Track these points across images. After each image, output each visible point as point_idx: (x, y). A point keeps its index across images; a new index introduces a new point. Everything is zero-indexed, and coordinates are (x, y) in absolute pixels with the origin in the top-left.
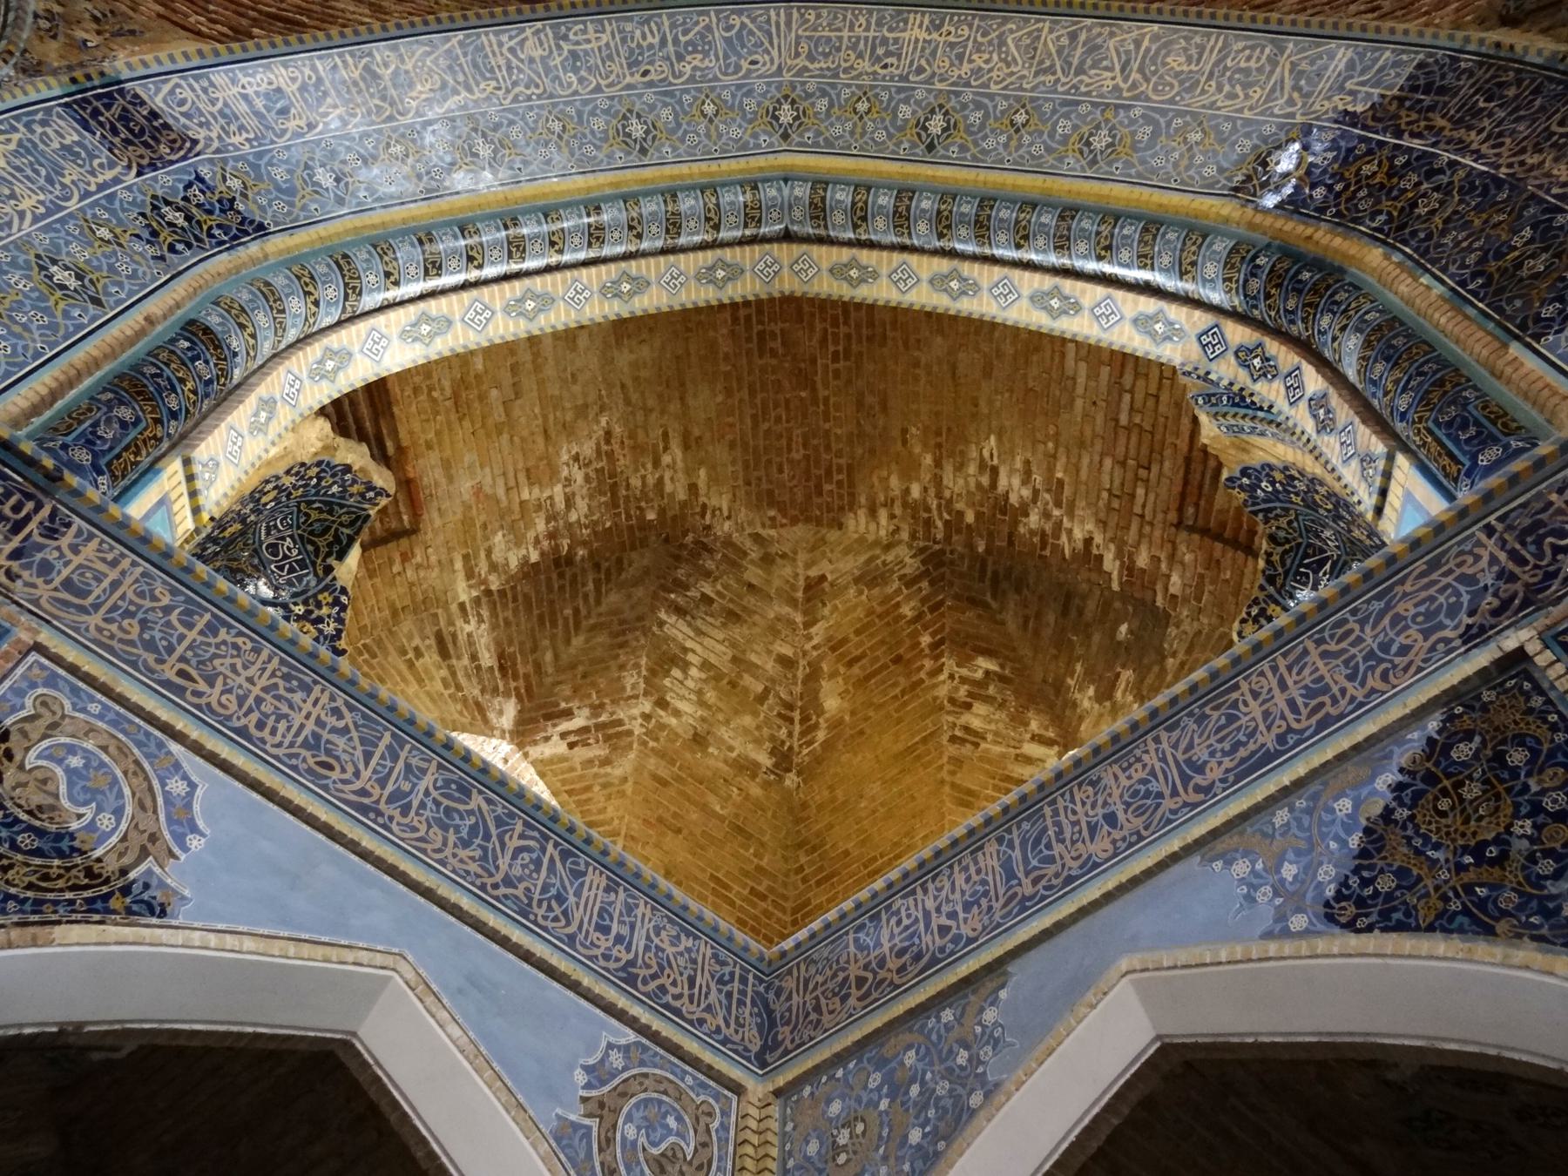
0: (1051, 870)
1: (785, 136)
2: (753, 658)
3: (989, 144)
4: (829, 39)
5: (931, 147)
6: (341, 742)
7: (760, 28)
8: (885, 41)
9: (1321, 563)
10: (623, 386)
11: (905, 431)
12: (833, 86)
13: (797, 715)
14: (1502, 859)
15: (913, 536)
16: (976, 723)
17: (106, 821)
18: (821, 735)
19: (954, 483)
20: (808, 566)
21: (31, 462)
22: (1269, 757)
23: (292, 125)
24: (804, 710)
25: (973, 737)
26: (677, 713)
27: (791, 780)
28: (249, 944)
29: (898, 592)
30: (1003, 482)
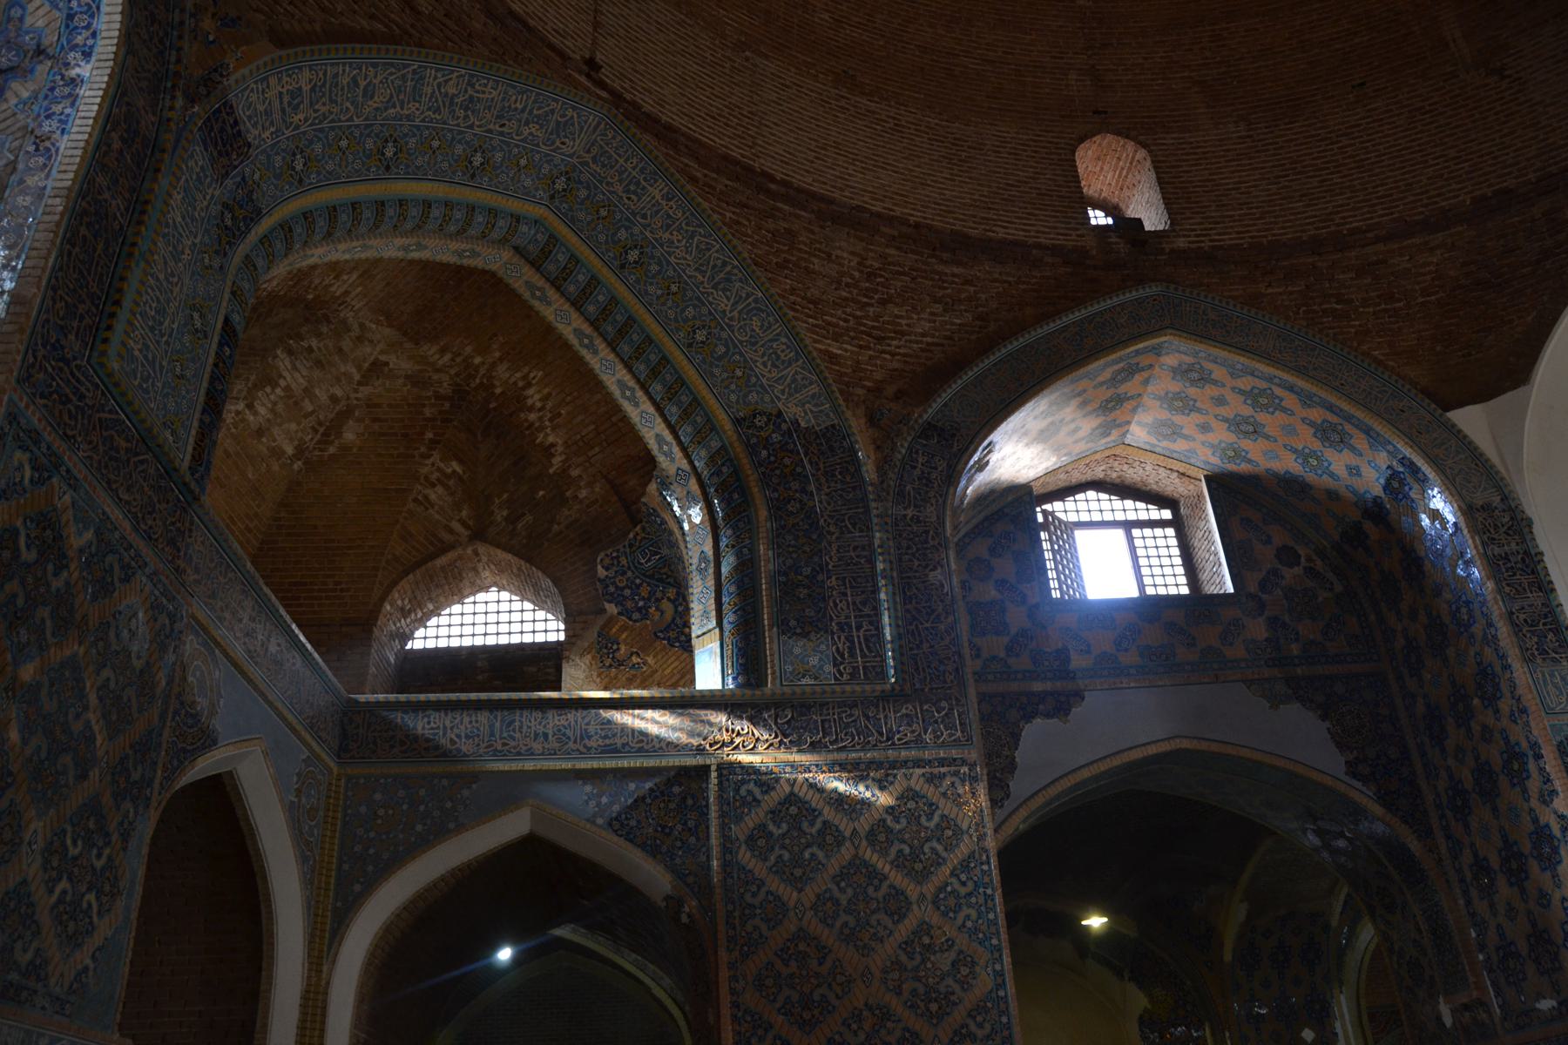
0: (513, 743)
1: (552, 197)
2: (317, 391)
3: (651, 289)
4: (610, 157)
5: (622, 266)
8: (638, 184)
9: (656, 553)
11: (495, 335)
12: (596, 188)
13: (322, 430)
14: (669, 835)
15: (457, 375)
16: (433, 497)
18: (332, 450)
19: (502, 371)
20: (382, 352)
22: (616, 751)
23: (296, 118)
24: (330, 431)
25: (427, 503)
26: (256, 413)
27: (298, 465)
29: (429, 398)
30: (531, 392)
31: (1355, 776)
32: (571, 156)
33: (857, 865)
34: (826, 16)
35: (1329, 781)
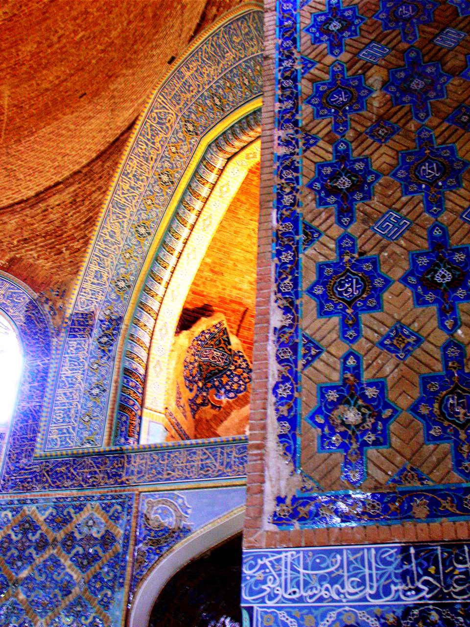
6: (208, 461)
7: (161, 109)
10: (251, 220)
17: (171, 519)
21: (116, 450)
23: (105, 278)
28: (210, 526)
32: (177, 115)
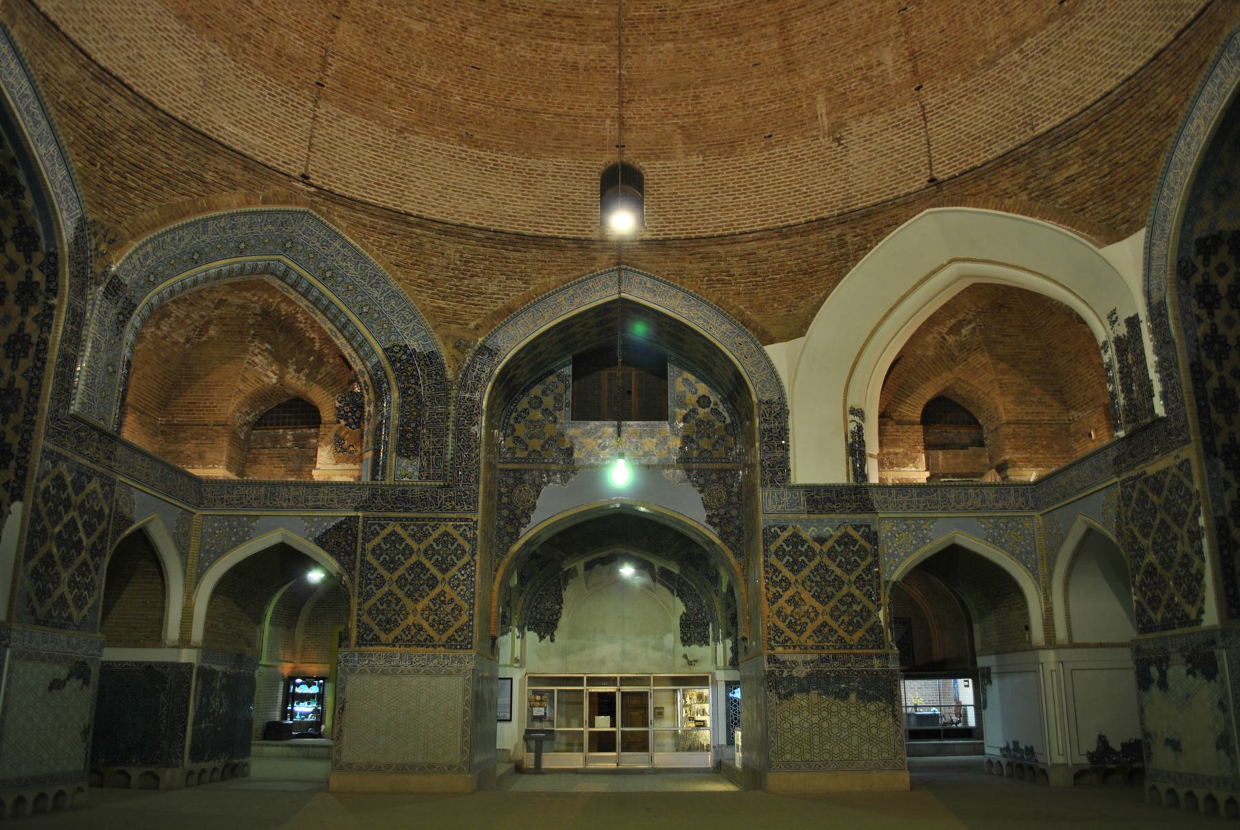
24: (203, 330)
25: (254, 364)
27: (188, 346)
31: (709, 523)
33: (419, 564)
34: (458, 98)
35: (695, 525)
